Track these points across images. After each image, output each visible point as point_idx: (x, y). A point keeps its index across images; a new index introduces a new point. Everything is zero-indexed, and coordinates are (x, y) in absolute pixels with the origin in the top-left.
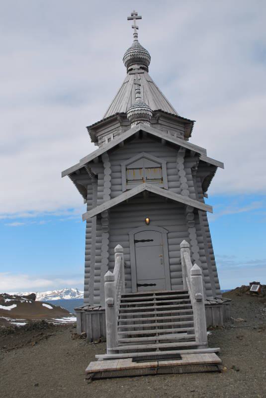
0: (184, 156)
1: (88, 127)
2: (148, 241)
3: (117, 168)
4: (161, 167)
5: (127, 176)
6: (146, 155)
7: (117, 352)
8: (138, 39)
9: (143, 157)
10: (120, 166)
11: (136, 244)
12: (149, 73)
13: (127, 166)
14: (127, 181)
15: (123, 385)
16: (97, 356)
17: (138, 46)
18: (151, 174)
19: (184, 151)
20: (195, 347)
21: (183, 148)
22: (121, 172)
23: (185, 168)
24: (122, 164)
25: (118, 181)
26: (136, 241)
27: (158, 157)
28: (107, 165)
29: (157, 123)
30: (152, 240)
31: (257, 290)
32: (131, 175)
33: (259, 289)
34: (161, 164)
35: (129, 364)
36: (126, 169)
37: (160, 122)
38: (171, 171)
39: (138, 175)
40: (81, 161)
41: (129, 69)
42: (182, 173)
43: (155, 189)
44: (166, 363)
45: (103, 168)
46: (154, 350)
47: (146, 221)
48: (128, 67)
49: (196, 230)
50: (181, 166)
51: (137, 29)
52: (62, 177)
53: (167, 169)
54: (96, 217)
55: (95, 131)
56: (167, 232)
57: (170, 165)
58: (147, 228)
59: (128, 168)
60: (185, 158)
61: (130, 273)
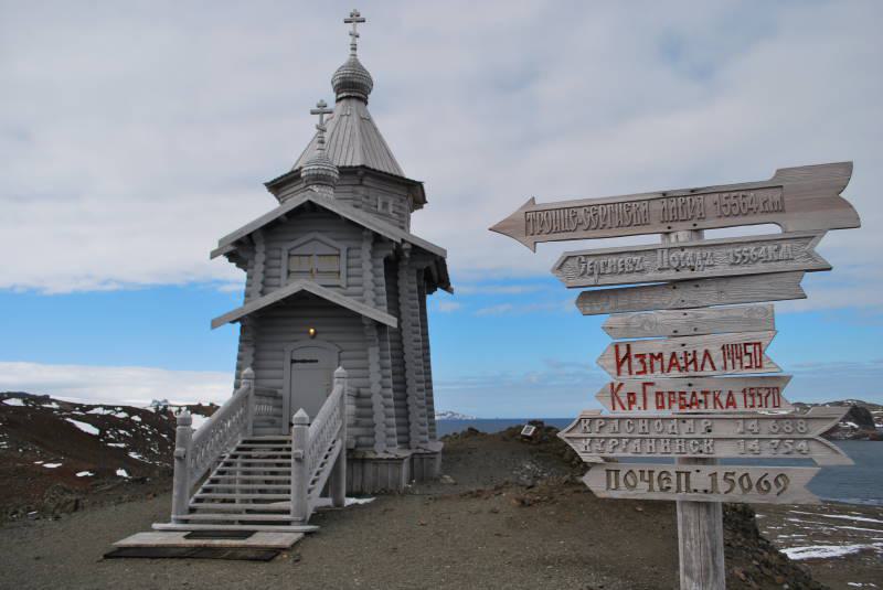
0: (372, 241)
1: (266, 184)
2: (311, 361)
3: (277, 253)
4: (339, 255)
5: (288, 266)
6: (319, 236)
7: (186, 521)
8: (357, 52)
9: (313, 240)
10: (280, 249)
11: (295, 365)
12: (369, 107)
13: (289, 250)
14: (289, 272)
15: (172, 568)
16: (156, 526)
17: (355, 65)
18: (324, 264)
19: (370, 234)
20: (288, 523)
21: (368, 230)
22: (280, 258)
25: (275, 272)
26: (293, 361)
27: (335, 239)
28: (260, 248)
29: (361, 185)
30: (317, 361)
31: (530, 434)
32: (295, 264)
33: (535, 432)
34: (339, 250)
35: (178, 539)
36: (289, 255)
37: (365, 183)
38: (352, 261)
39: (305, 264)
40: (221, 242)
41: (340, 96)
42: (367, 266)
43: (314, 287)
44: (217, 542)
45: (255, 252)
46: (232, 522)
47: (309, 332)
48: (338, 94)
49: (381, 350)
51: (357, 36)
53: (348, 258)
54: (238, 325)
55: (276, 187)
57: (353, 253)
58: (314, 342)
59: (293, 252)
60: (373, 244)
61: (281, 407)
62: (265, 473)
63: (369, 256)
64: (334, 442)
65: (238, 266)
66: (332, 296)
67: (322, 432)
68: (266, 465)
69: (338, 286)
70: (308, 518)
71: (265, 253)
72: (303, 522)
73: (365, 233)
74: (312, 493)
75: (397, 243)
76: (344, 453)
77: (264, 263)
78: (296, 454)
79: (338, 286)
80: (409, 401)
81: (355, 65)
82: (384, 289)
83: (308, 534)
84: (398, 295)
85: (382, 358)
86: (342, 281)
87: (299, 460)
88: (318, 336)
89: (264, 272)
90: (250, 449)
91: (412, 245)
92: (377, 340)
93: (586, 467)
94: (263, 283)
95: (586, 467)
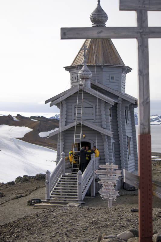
3: (70, 107)
4: (93, 108)
10: (72, 105)
17: (99, 9)
22: (72, 109)
23: (105, 108)
24: (73, 105)
25: (70, 114)
28: (65, 106)
34: (93, 106)
42: (103, 113)
50: (103, 108)
52: (45, 104)
56: (94, 143)
60: (105, 104)
62: (69, 187)
63: (104, 109)
64: (91, 177)
65: (57, 107)
66: (95, 96)
67: (86, 175)
68: (69, 184)
69: (93, 119)
70: (82, 199)
71: (66, 107)
72: (81, 201)
73: (101, 101)
74: (84, 193)
75: (113, 106)
76: (95, 180)
77: (66, 111)
78: (78, 183)
79: (93, 119)
80: (121, 159)
81: (99, 9)
82: (110, 120)
83: (82, 204)
84: (117, 118)
85: (109, 146)
86: (94, 118)
87: (79, 184)
88: (86, 138)
89: (66, 115)
90: (65, 179)
91: (122, 98)
92: (107, 140)
93: (100, 195)
94: (66, 118)
95: (100, 195)
